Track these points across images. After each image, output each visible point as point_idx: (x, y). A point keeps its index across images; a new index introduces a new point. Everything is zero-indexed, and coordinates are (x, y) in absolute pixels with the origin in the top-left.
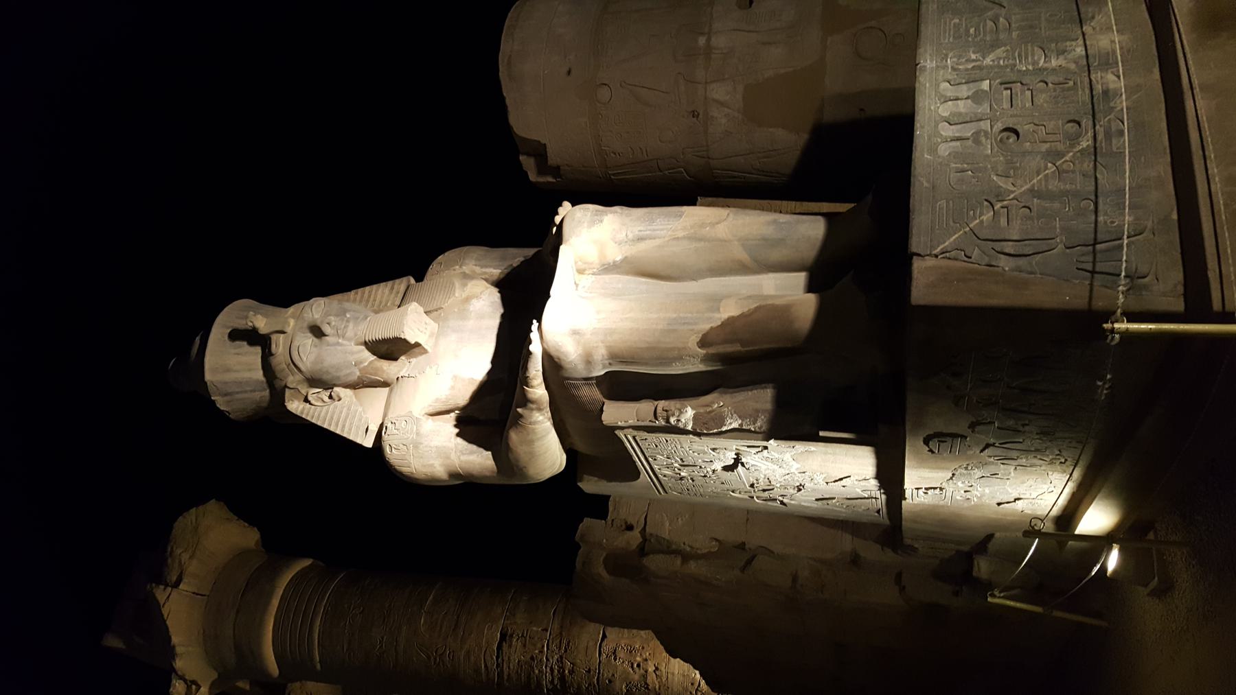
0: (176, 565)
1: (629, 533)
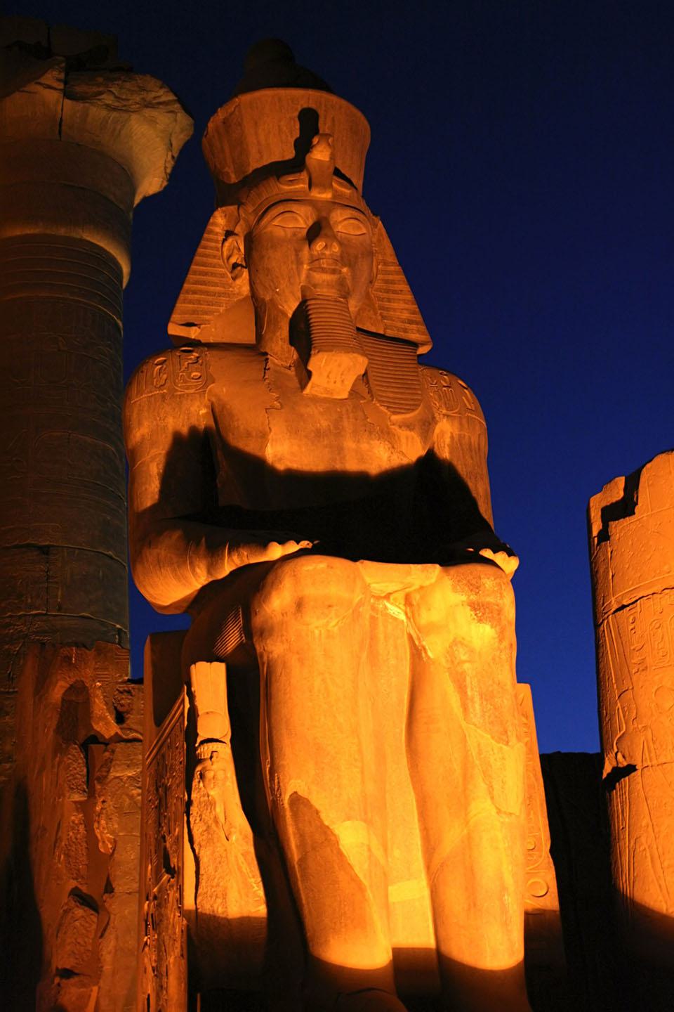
0: (95, 89)
1: (111, 719)
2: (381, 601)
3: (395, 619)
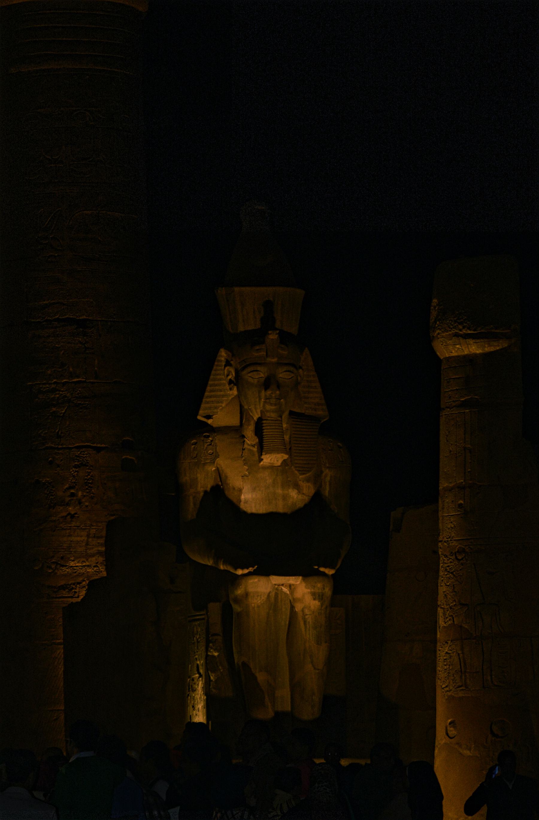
3: (285, 593)
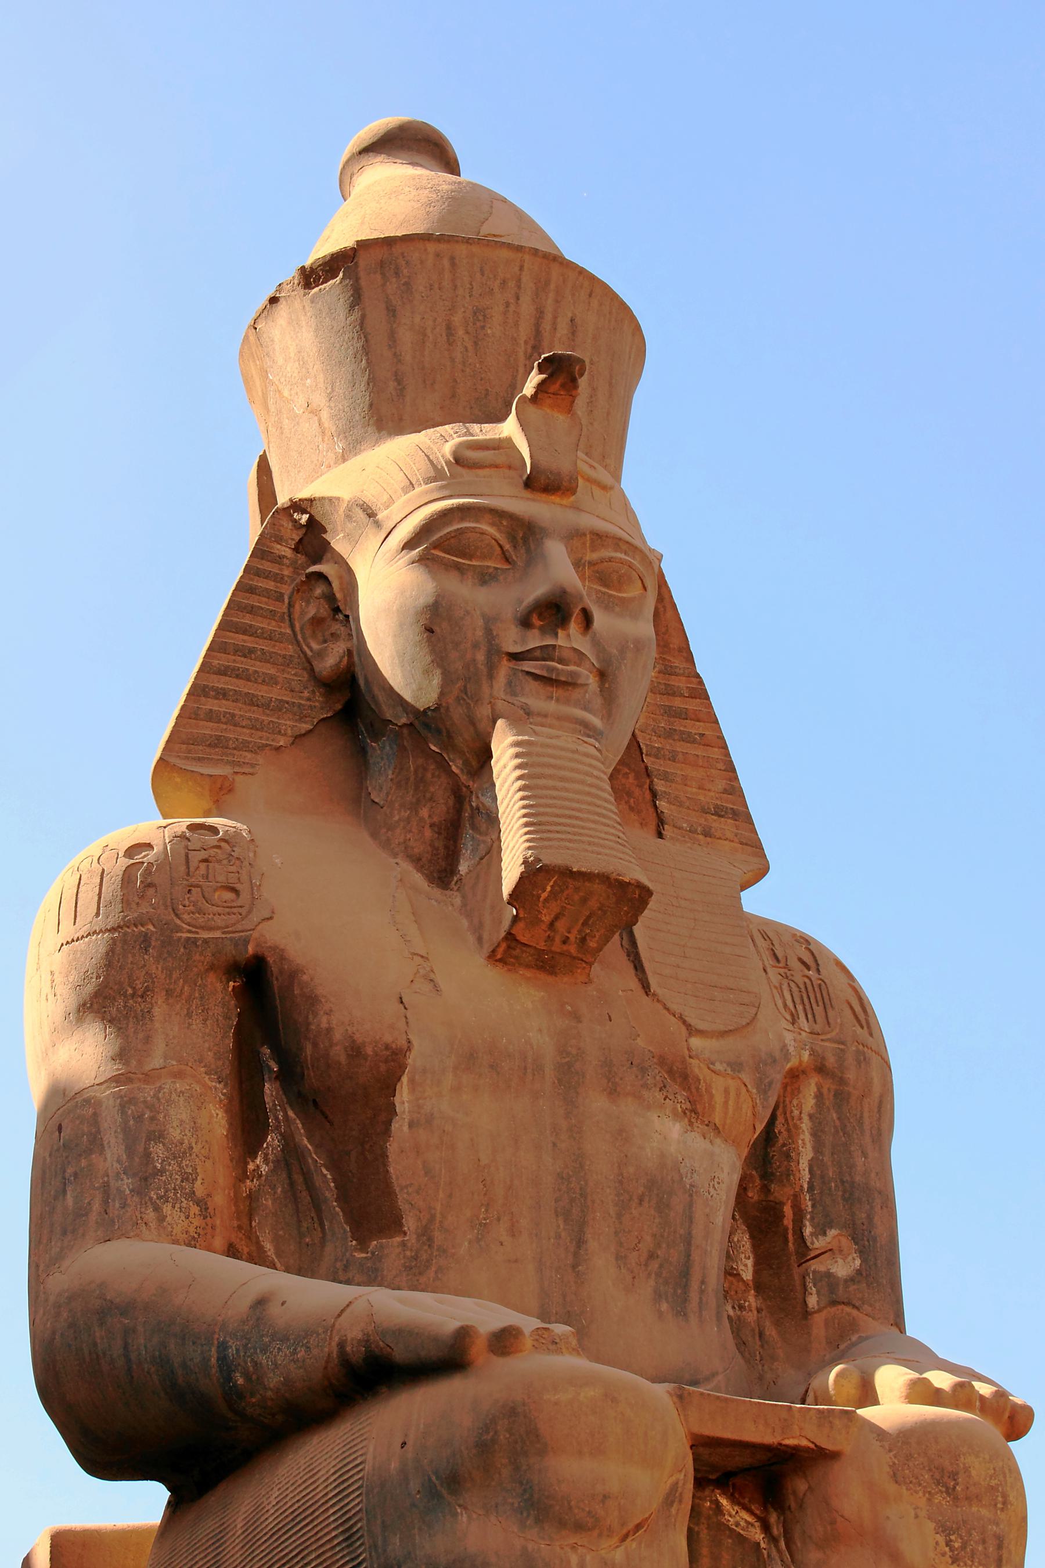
2: (707, 1492)
